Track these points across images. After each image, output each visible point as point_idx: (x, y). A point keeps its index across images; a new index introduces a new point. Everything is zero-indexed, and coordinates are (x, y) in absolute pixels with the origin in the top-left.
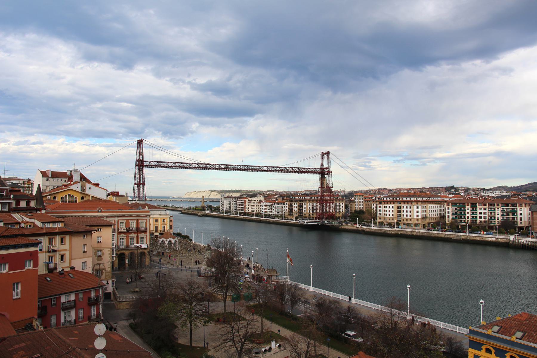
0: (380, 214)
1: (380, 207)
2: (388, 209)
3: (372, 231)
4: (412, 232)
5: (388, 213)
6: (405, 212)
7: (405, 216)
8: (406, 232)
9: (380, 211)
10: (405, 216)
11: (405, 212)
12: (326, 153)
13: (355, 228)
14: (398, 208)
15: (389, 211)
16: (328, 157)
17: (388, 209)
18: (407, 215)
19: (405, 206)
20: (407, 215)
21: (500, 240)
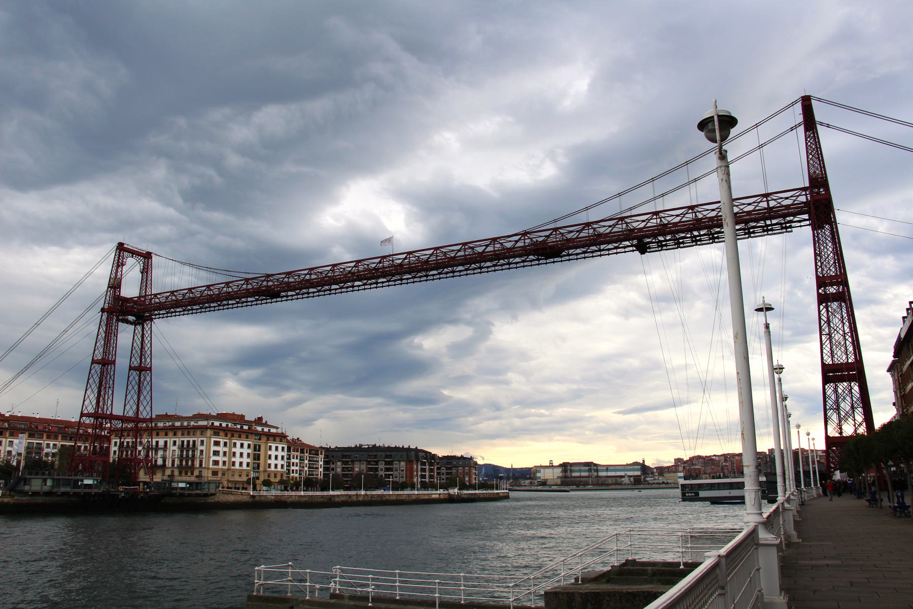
0: (216, 463)
1: (217, 443)
2: (238, 450)
3: (303, 499)
4: (357, 495)
5: (237, 460)
6: (273, 457)
7: (273, 468)
8: (350, 496)
9: (216, 453)
10: (273, 468)
11: (273, 457)
12: (133, 253)
13: (246, 498)
14: (255, 450)
15: (241, 454)
16: (146, 271)
17: (238, 450)
18: (276, 466)
19: (274, 446)
20: (276, 466)
21: (442, 497)
